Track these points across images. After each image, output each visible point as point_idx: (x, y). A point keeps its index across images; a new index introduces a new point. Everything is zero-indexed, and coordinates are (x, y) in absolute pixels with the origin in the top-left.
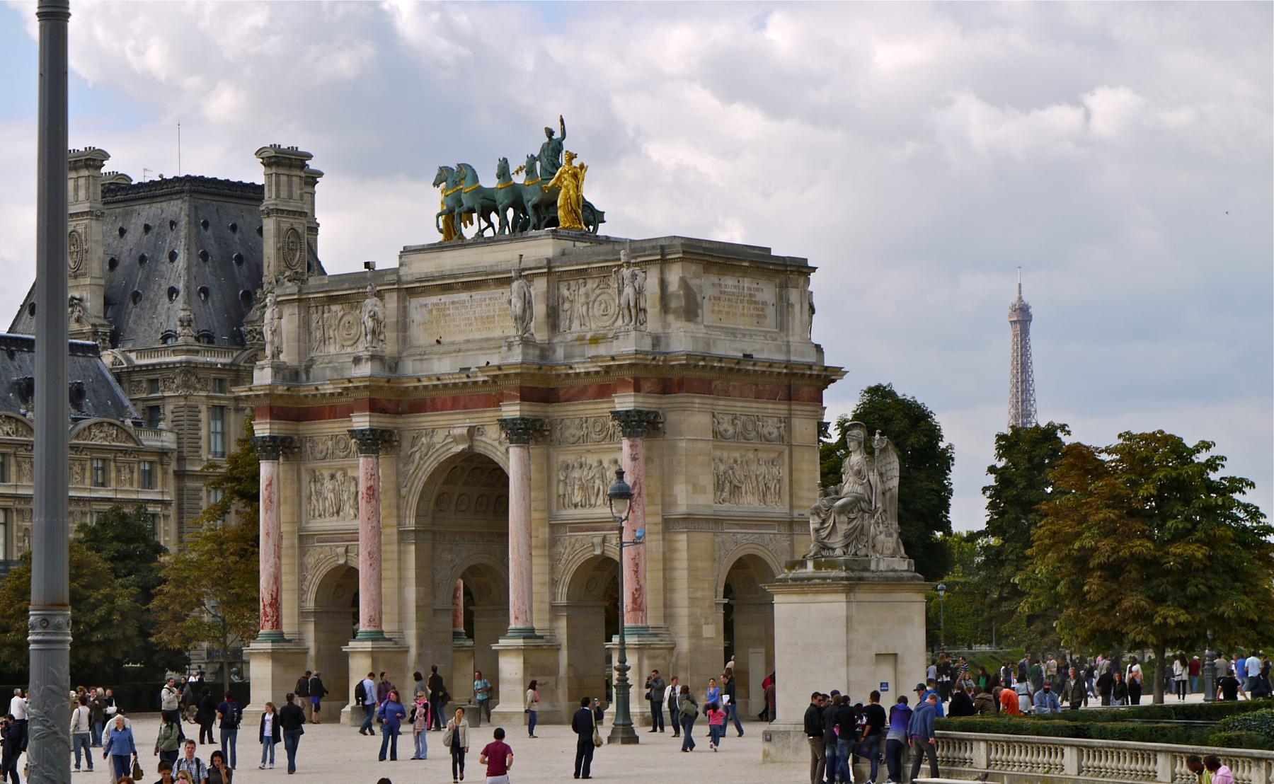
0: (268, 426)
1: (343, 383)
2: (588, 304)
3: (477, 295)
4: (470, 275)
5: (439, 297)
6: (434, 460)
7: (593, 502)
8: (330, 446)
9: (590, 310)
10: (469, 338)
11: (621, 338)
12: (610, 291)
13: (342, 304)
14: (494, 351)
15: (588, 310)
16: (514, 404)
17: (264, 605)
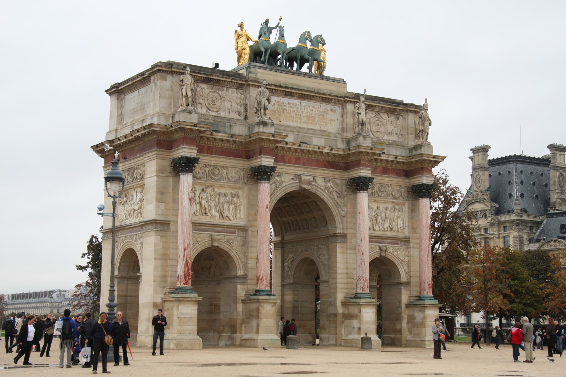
0: (196, 151)
1: (268, 136)
2: (370, 123)
3: (305, 103)
4: (307, 91)
5: (280, 98)
6: (283, 191)
7: (374, 227)
8: (207, 171)
9: (372, 128)
10: (299, 125)
11: (426, 147)
12: (381, 120)
13: (209, 84)
14: (321, 137)
15: (370, 127)
16: (369, 170)
17: (188, 269)
